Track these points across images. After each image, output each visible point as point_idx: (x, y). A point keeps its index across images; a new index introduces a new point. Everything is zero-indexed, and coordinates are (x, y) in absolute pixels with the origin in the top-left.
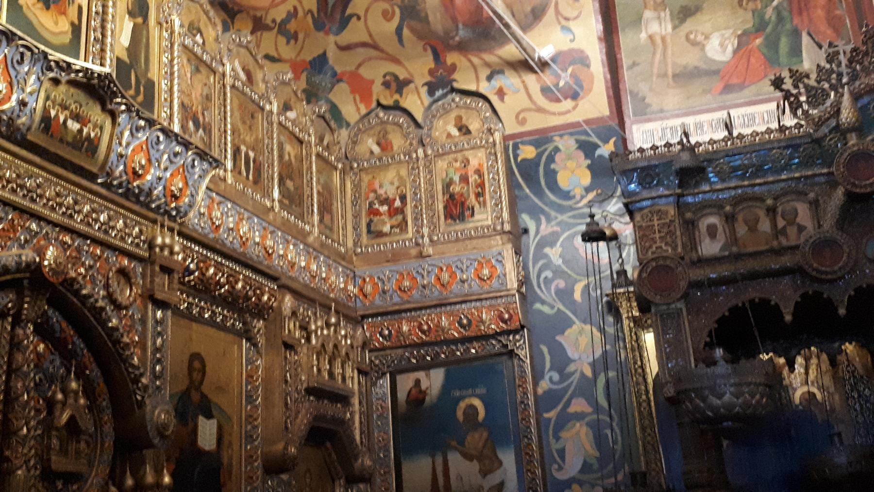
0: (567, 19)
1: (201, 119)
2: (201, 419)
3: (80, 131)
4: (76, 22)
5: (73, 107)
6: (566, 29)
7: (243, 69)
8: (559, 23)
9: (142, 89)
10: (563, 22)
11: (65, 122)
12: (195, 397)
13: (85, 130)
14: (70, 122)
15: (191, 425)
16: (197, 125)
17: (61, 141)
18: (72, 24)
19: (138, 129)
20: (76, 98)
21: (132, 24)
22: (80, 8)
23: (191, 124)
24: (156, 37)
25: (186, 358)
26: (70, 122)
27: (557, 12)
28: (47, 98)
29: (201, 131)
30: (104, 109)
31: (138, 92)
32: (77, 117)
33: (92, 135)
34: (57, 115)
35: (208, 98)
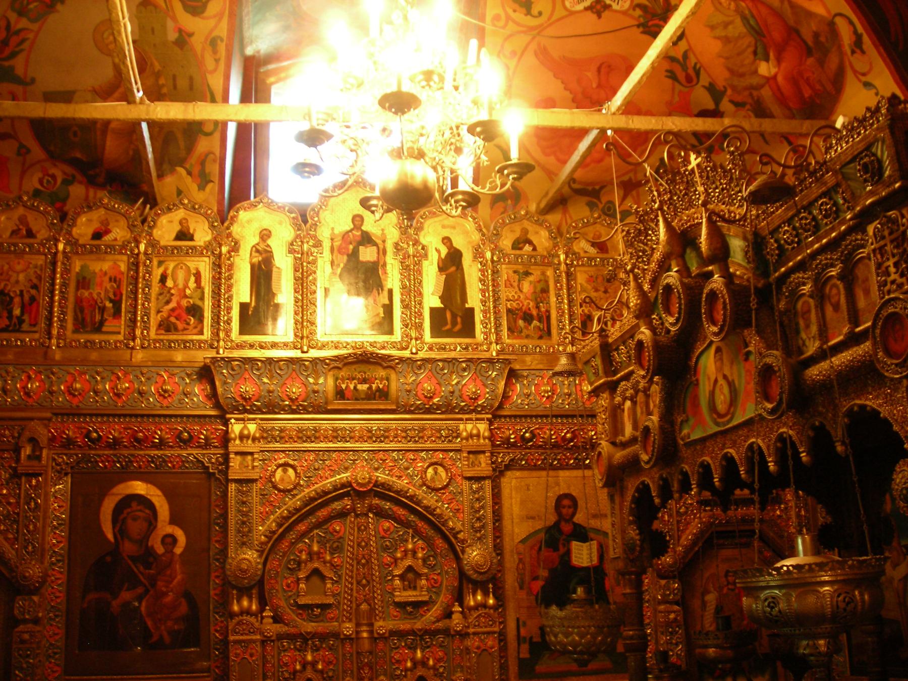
0: (864, 75)
1: (534, 312)
2: (575, 544)
3: (370, 388)
4: (387, 302)
5: (359, 376)
6: (867, 85)
7: (593, 245)
8: (860, 80)
9: (459, 320)
10: (863, 79)
11: (355, 388)
12: (566, 528)
13: (374, 386)
14: (359, 387)
15: (562, 550)
16: (528, 318)
17: (357, 399)
18: (384, 306)
19: (420, 368)
20: (358, 370)
21: (444, 276)
22: (390, 292)
23: (521, 323)
24: (472, 272)
25: (552, 503)
26: (359, 387)
27: (855, 72)
28: (337, 379)
29: (535, 323)
30: (385, 368)
31: (454, 323)
32: (364, 381)
33: (381, 386)
34: (347, 387)
35: (545, 291)
